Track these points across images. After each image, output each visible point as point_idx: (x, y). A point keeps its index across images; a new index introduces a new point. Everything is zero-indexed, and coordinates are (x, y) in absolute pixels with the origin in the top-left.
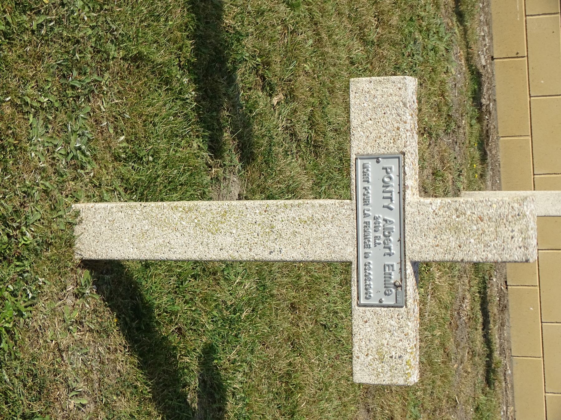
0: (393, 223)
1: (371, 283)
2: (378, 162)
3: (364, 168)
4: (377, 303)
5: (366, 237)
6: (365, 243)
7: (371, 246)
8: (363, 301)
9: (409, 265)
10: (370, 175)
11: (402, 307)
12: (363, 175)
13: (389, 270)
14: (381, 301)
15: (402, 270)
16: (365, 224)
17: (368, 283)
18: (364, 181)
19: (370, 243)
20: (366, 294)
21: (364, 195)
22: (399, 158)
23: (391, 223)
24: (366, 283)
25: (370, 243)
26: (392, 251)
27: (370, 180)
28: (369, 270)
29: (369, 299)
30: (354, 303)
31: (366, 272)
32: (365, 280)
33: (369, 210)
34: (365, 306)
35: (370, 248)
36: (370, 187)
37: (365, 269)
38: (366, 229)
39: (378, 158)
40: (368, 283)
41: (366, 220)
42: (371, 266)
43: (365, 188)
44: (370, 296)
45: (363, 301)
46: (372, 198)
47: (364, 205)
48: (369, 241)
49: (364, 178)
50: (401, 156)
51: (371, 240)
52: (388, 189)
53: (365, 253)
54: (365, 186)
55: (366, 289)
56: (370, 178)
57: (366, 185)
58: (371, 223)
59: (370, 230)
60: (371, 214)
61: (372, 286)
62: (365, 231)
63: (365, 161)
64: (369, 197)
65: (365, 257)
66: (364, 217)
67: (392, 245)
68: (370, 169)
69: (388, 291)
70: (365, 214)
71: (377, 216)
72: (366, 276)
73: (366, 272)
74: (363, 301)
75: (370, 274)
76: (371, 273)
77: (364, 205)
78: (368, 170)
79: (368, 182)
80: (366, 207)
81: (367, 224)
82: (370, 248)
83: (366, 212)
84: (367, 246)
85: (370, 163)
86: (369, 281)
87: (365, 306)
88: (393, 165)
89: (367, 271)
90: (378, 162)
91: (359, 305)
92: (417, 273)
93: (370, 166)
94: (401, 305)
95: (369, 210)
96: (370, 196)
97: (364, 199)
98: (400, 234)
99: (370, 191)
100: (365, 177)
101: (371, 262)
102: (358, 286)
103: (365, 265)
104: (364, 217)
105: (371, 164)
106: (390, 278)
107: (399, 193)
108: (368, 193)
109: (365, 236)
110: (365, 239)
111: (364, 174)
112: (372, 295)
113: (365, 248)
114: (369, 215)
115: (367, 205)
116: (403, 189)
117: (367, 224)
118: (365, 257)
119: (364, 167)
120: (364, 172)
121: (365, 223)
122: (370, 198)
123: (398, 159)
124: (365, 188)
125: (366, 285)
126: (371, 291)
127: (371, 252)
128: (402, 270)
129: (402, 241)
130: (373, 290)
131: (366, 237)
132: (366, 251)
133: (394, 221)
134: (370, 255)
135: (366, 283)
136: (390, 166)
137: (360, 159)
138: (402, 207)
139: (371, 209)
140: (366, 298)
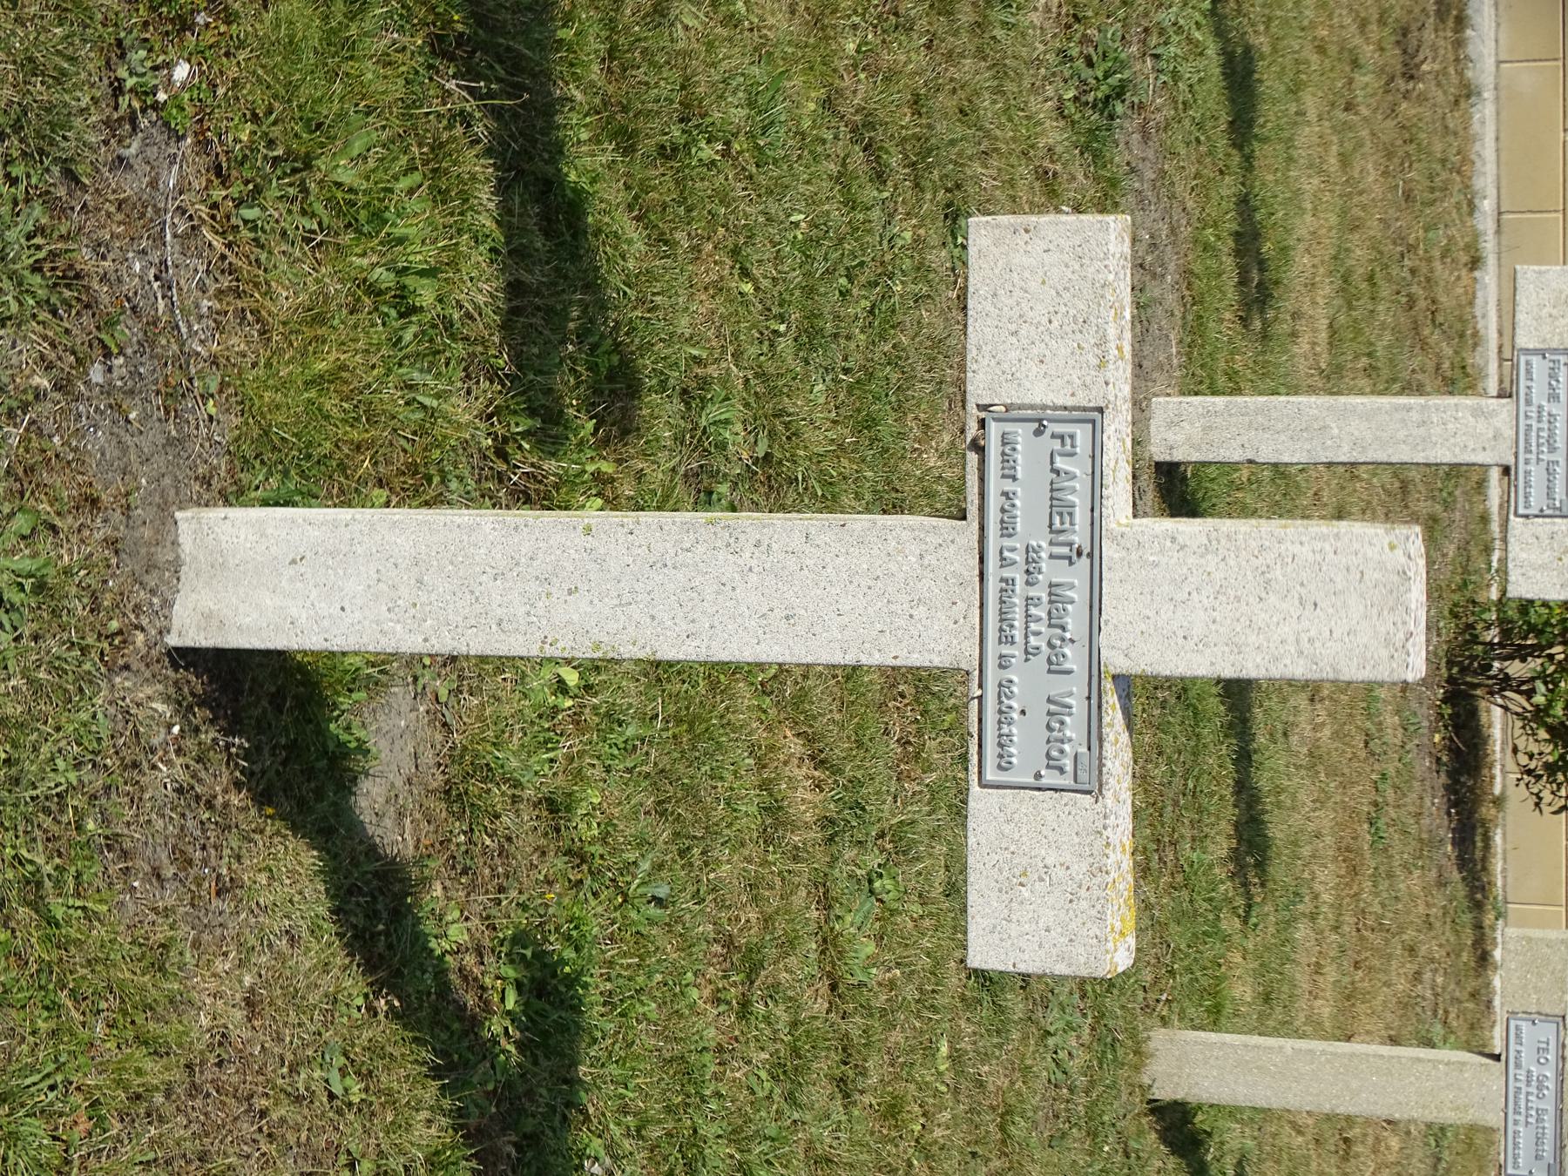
1: (1015, 731)
3: (1004, 444)
4: (1030, 780)
6: (1001, 630)
7: (1017, 639)
9: (1108, 685)
10: (1020, 461)
12: (1003, 462)
13: (1062, 523)
14: (1038, 776)
17: (1005, 730)
18: (1003, 476)
20: (1001, 756)
21: (1003, 510)
22: (1093, 422)
24: (999, 729)
26: (1068, 733)
27: (1019, 475)
29: (1006, 770)
30: (974, 777)
31: (1001, 702)
32: (1000, 722)
33: (1013, 550)
35: (1013, 643)
36: (1019, 489)
39: (1040, 421)
40: (1005, 730)
42: (1015, 689)
43: (1005, 494)
47: (1002, 536)
48: (1012, 626)
49: (1003, 468)
51: (1016, 623)
52: (1062, 538)
53: (1001, 656)
54: (1006, 489)
55: (1001, 745)
56: (1019, 468)
57: (1008, 486)
58: (1018, 582)
59: (1016, 600)
60: (1018, 558)
61: (1015, 739)
62: (1002, 602)
65: (1001, 666)
66: (1002, 566)
67: (1070, 621)
68: (1019, 447)
69: (1056, 655)
70: (1003, 559)
71: (1035, 544)
72: (1000, 712)
73: (1001, 702)
74: (990, 775)
77: (1002, 536)
78: (1014, 449)
79: (1014, 478)
80: (1007, 542)
82: (1013, 643)
83: (1006, 554)
85: (1020, 431)
86: (1009, 724)
88: (1082, 433)
89: (1006, 701)
92: (1126, 697)
93: (1020, 439)
94: (1086, 787)
95: (1013, 550)
96: (1019, 513)
97: (1002, 521)
98: (1089, 732)
99: (1018, 502)
101: (1015, 679)
102: (982, 479)
103: (1000, 685)
104: (1002, 566)
107: (1089, 698)
108: (1013, 505)
109: (1001, 613)
110: (1001, 620)
112: (1014, 760)
113: (1000, 642)
115: (1010, 536)
118: (1001, 666)
120: (1003, 454)
121: (1002, 580)
122: (1018, 520)
123: (1090, 426)
125: (1000, 736)
126: (1013, 750)
127: (1017, 653)
132: (1005, 652)
134: (1013, 660)
135: (999, 729)
139: (1018, 545)
140: (1000, 767)
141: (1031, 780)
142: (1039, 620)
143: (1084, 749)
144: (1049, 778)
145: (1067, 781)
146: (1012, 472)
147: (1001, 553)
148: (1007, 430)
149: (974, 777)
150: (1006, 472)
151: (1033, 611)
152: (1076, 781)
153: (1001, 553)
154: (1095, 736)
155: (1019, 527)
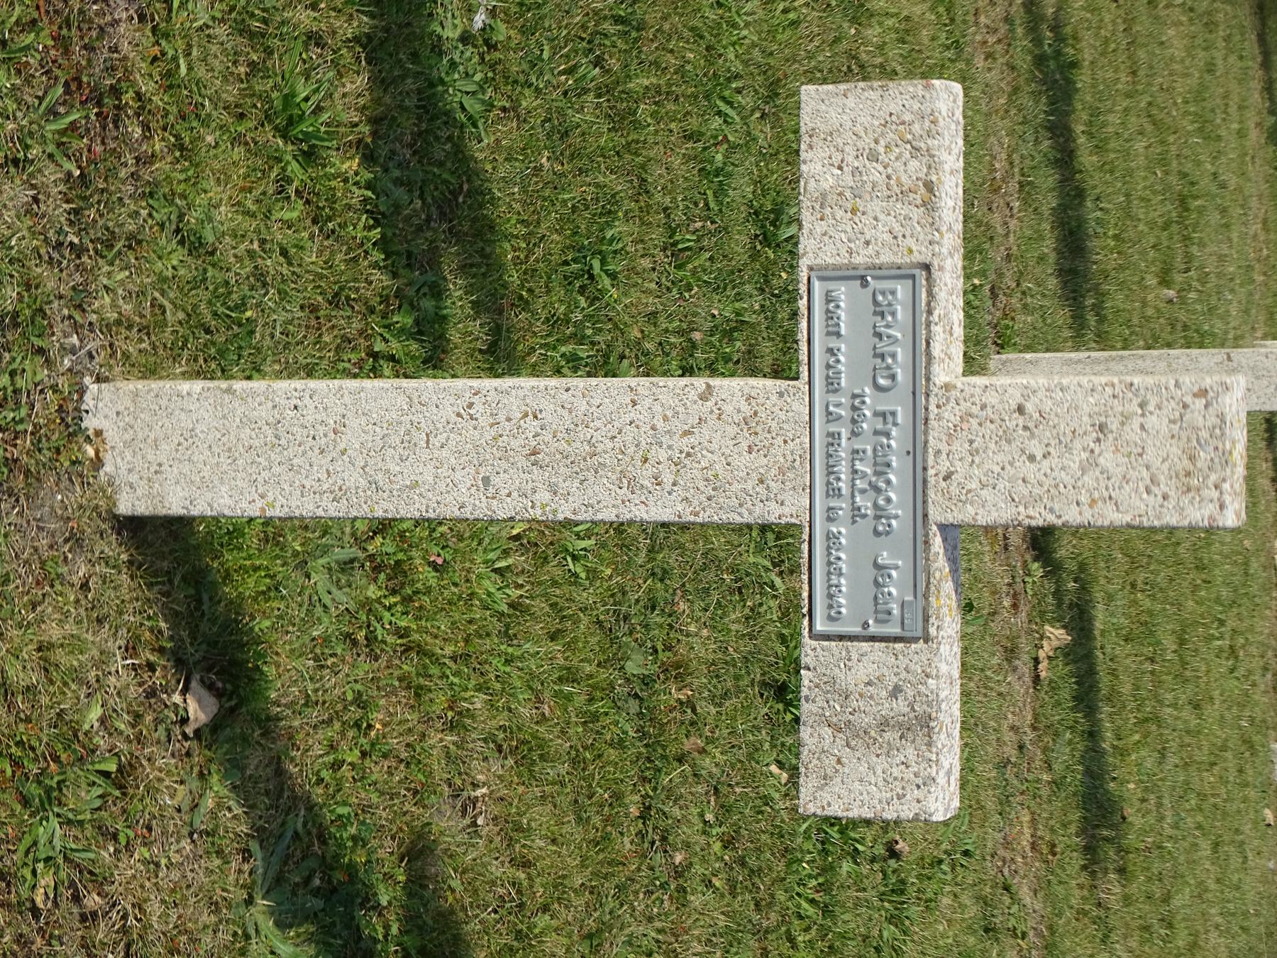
0: (897, 340)
1: (843, 581)
2: (865, 284)
3: (828, 301)
4: (856, 630)
5: (830, 470)
6: (828, 483)
7: (844, 492)
8: (822, 625)
10: (843, 317)
11: (916, 640)
14: (866, 625)
15: (920, 544)
16: (830, 440)
17: (834, 582)
18: (829, 334)
19: (841, 484)
20: (830, 607)
21: (828, 367)
22: (913, 277)
23: (891, 340)
25: (841, 484)
27: (843, 332)
28: (838, 550)
29: (837, 619)
32: (829, 573)
34: (827, 637)
35: (840, 495)
36: (843, 347)
37: (829, 548)
38: (831, 449)
41: (831, 430)
42: (843, 541)
43: (831, 351)
44: (840, 613)
45: (819, 627)
46: (847, 312)
47: (828, 392)
48: (839, 479)
49: (828, 326)
50: (921, 276)
51: (843, 476)
53: (830, 509)
54: (831, 345)
55: (830, 596)
56: (842, 325)
57: (833, 343)
59: (843, 455)
60: (843, 413)
61: (844, 589)
63: (831, 285)
64: (840, 373)
65: (829, 519)
66: (828, 421)
68: (842, 304)
72: (829, 563)
73: (830, 554)
74: (819, 627)
75: (839, 559)
76: (843, 556)
77: (828, 392)
78: (838, 307)
79: (838, 335)
80: (833, 398)
81: (833, 437)
83: (831, 408)
84: (832, 492)
87: (827, 637)
90: (865, 284)
91: (814, 636)
93: (843, 297)
95: (838, 405)
97: (828, 377)
99: (842, 359)
100: (830, 322)
101: (843, 530)
103: (828, 538)
104: (828, 421)
105: (841, 291)
106: (890, 613)
108: (838, 361)
109: (829, 466)
110: (829, 473)
111: (829, 315)
112: (843, 610)
113: (828, 495)
114: (840, 417)
115: (836, 391)
116: (922, 356)
117: (833, 437)
118: (829, 519)
119: (829, 298)
120: (828, 311)
123: (910, 282)
124: (831, 351)
126: (842, 601)
128: (920, 544)
129: (920, 487)
130: (848, 597)
131: (830, 470)
132: (831, 505)
133: (899, 335)
135: (829, 580)
136: (892, 408)
137: (821, 279)
138: (920, 539)
140: (830, 618)
141: (859, 629)
142: (864, 475)
143: (909, 598)
144: (874, 629)
145: (895, 630)
146: (835, 329)
147: (827, 407)
148: (831, 288)
149: (806, 632)
150: (830, 329)
151: (859, 466)
152: (903, 629)
153: (827, 407)
154: (922, 587)
155: (843, 383)
